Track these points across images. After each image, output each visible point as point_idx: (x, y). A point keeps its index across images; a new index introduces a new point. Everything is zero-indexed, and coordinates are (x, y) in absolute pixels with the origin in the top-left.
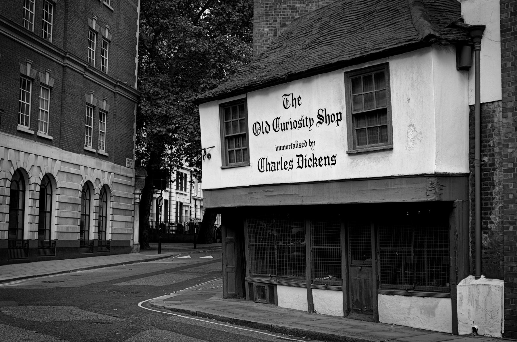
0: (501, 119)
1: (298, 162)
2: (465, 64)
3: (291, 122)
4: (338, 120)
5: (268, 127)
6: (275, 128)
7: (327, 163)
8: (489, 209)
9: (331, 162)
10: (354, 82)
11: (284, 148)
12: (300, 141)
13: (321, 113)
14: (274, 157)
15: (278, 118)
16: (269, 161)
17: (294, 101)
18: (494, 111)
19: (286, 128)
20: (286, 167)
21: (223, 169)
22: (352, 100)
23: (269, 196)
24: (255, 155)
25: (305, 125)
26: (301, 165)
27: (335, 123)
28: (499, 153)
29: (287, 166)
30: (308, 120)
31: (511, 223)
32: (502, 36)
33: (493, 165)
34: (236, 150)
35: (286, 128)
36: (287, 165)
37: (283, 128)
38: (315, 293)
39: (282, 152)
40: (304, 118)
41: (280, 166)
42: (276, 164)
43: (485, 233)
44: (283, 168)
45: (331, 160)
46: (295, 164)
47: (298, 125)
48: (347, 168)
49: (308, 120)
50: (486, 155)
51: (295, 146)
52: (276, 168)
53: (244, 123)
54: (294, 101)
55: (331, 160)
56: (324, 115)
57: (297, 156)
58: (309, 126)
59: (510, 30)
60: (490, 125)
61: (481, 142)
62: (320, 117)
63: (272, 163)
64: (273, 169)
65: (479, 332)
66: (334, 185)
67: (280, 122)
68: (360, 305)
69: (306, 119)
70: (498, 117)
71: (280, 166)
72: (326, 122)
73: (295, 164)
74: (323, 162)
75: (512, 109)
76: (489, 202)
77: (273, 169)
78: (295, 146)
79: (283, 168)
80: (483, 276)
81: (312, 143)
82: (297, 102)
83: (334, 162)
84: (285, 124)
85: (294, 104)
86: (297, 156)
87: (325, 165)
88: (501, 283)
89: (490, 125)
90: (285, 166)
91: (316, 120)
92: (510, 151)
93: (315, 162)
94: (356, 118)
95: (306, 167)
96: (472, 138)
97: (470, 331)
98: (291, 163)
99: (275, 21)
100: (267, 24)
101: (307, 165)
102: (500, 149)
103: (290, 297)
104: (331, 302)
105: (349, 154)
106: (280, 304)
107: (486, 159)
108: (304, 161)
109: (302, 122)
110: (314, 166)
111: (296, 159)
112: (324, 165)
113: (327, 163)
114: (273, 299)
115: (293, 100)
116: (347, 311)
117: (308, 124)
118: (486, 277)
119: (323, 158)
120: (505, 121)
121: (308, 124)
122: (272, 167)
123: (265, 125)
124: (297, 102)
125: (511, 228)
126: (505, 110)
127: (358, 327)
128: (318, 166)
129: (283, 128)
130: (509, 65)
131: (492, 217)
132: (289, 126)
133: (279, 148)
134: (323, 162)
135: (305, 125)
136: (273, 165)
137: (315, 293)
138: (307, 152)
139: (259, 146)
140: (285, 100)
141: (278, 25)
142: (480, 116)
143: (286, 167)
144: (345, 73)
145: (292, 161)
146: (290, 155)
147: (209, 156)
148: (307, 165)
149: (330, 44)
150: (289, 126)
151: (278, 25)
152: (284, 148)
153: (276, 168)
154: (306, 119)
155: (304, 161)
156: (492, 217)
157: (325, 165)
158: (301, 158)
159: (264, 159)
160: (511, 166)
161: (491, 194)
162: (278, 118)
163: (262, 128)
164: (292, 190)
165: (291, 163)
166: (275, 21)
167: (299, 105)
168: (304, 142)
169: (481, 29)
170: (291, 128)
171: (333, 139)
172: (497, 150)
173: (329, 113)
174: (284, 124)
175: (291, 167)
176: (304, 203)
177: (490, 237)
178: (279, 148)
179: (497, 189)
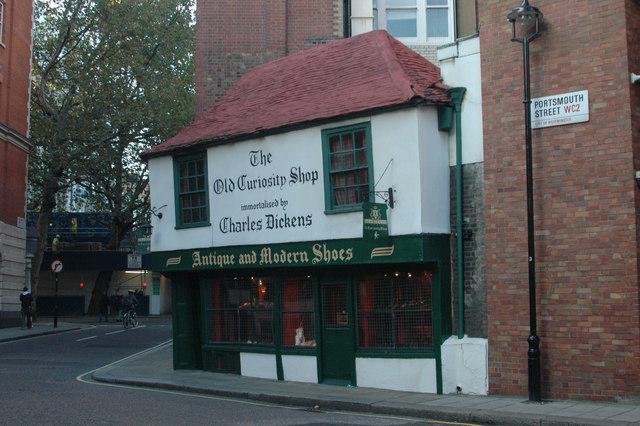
0: (483, 181)
2: (445, 126)
5: (232, 186)
8: (472, 269)
9: (306, 223)
10: (331, 142)
13: (294, 171)
14: (239, 216)
16: (234, 221)
18: (475, 173)
21: (177, 228)
22: (330, 160)
24: (215, 216)
26: (271, 225)
28: (481, 214)
29: (255, 226)
31: (494, 283)
32: (483, 99)
33: (475, 225)
34: (192, 209)
36: (254, 226)
38: (285, 359)
40: (275, 176)
41: (246, 226)
43: (468, 293)
45: (306, 221)
46: (264, 224)
50: (467, 216)
51: (265, 205)
53: (202, 182)
55: (306, 221)
59: (491, 93)
60: (471, 186)
61: (463, 202)
62: (293, 176)
65: (464, 391)
67: (246, 180)
68: (336, 368)
70: (480, 178)
71: (246, 226)
73: (264, 224)
74: (296, 222)
75: (494, 171)
76: (471, 263)
78: (265, 205)
80: (465, 336)
81: (284, 203)
82: (266, 159)
88: (484, 342)
89: (471, 186)
91: (289, 178)
92: (493, 212)
93: (287, 222)
94: (332, 178)
96: (453, 199)
97: (454, 390)
99: (219, 70)
100: (210, 73)
102: (482, 209)
103: (256, 366)
104: (303, 369)
105: (326, 213)
106: (244, 372)
107: (467, 220)
111: (265, 220)
112: (297, 226)
114: (236, 368)
116: (323, 375)
118: (469, 336)
120: (487, 182)
122: (237, 227)
123: (229, 183)
124: (266, 159)
125: (494, 287)
126: (487, 171)
127: (335, 392)
130: (490, 128)
131: (474, 277)
133: (244, 208)
134: (296, 222)
137: (285, 359)
138: (278, 212)
141: (222, 76)
142: (460, 179)
144: (323, 131)
146: (259, 215)
147: (160, 216)
149: (299, 99)
150: (257, 184)
151: (222, 76)
156: (474, 277)
160: (493, 226)
161: (473, 254)
163: (224, 186)
166: (219, 70)
169: (460, 93)
171: (311, 198)
172: (478, 210)
173: (304, 171)
177: (473, 297)
178: (244, 208)
179: (479, 249)
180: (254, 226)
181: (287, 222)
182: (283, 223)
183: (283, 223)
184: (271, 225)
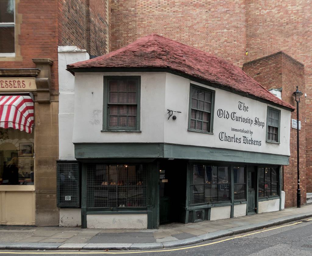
1: (244, 140)
3: (242, 118)
4: (263, 126)
6: (232, 118)
7: (257, 144)
9: (259, 144)
11: (236, 130)
12: (246, 129)
13: (256, 119)
14: (231, 134)
15: (235, 113)
16: (227, 135)
17: (245, 108)
19: (238, 120)
20: (237, 141)
23: (225, 156)
25: (249, 122)
26: (245, 142)
27: (262, 127)
30: (250, 121)
35: (238, 120)
36: (237, 140)
37: (237, 120)
39: (235, 132)
41: (233, 140)
42: (231, 138)
44: (235, 141)
45: (259, 143)
46: (242, 141)
47: (245, 121)
48: (264, 148)
49: (250, 121)
51: (242, 131)
52: (231, 140)
54: (245, 108)
55: (259, 143)
56: (258, 121)
57: (244, 137)
58: (250, 124)
62: (256, 121)
63: (228, 137)
64: (229, 140)
66: (259, 155)
67: (235, 115)
69: (250, 119)
71: (233, 140)
72: (258, 125)
74: (256, 143)
77: (229, 140)
78: (242, 131)
79: (235, 141)
81: (251, 133)
82: (246, 109)
83: (260, 144)
84: (239, 118)
85: (244, 109)
86: (244, 137)
87: (257, 145)
90: (236, 140)
93: (252, 142)
95: (248, 143)
98: (240, 140)
101: (248, 143)
108: (247, 140)
109: (247, 120)
110: (251, 144)
111: (242, 138)
113: (257, 144)
115: (244, 107)
117: (250, 122)
119: (256, 141)
121: (250, 122)
128: (254, 144)
129: (237, 120)
132: (240, 119)
133: (233, 130)
135: (249, 122)
136: (229, 138)
138: (249, 136)
139: (220, 124)
140: (240, 105)
143: (237, 141)
145: (240, 139)
148: (248, 143)
150: (240, 119)
152: (236, 130)
153: (231, 140)
154: (250, 119)
155: (247, 140)
157: (257, 145)
158: (245, 139)
159: (223, 133)
162: (235, 113)
164: (240, 154)
165: (240, 140)
167: (247, 111)
168: (247, 131)
170: (242, 121)
174: (238, 117)
175: (240, 142)
176: (245, 162)
178: (233, 130)
180: (237, 140)
181: (252, 142)
182: (250, 142)
183: (250, 142)
184: (245, 142)
